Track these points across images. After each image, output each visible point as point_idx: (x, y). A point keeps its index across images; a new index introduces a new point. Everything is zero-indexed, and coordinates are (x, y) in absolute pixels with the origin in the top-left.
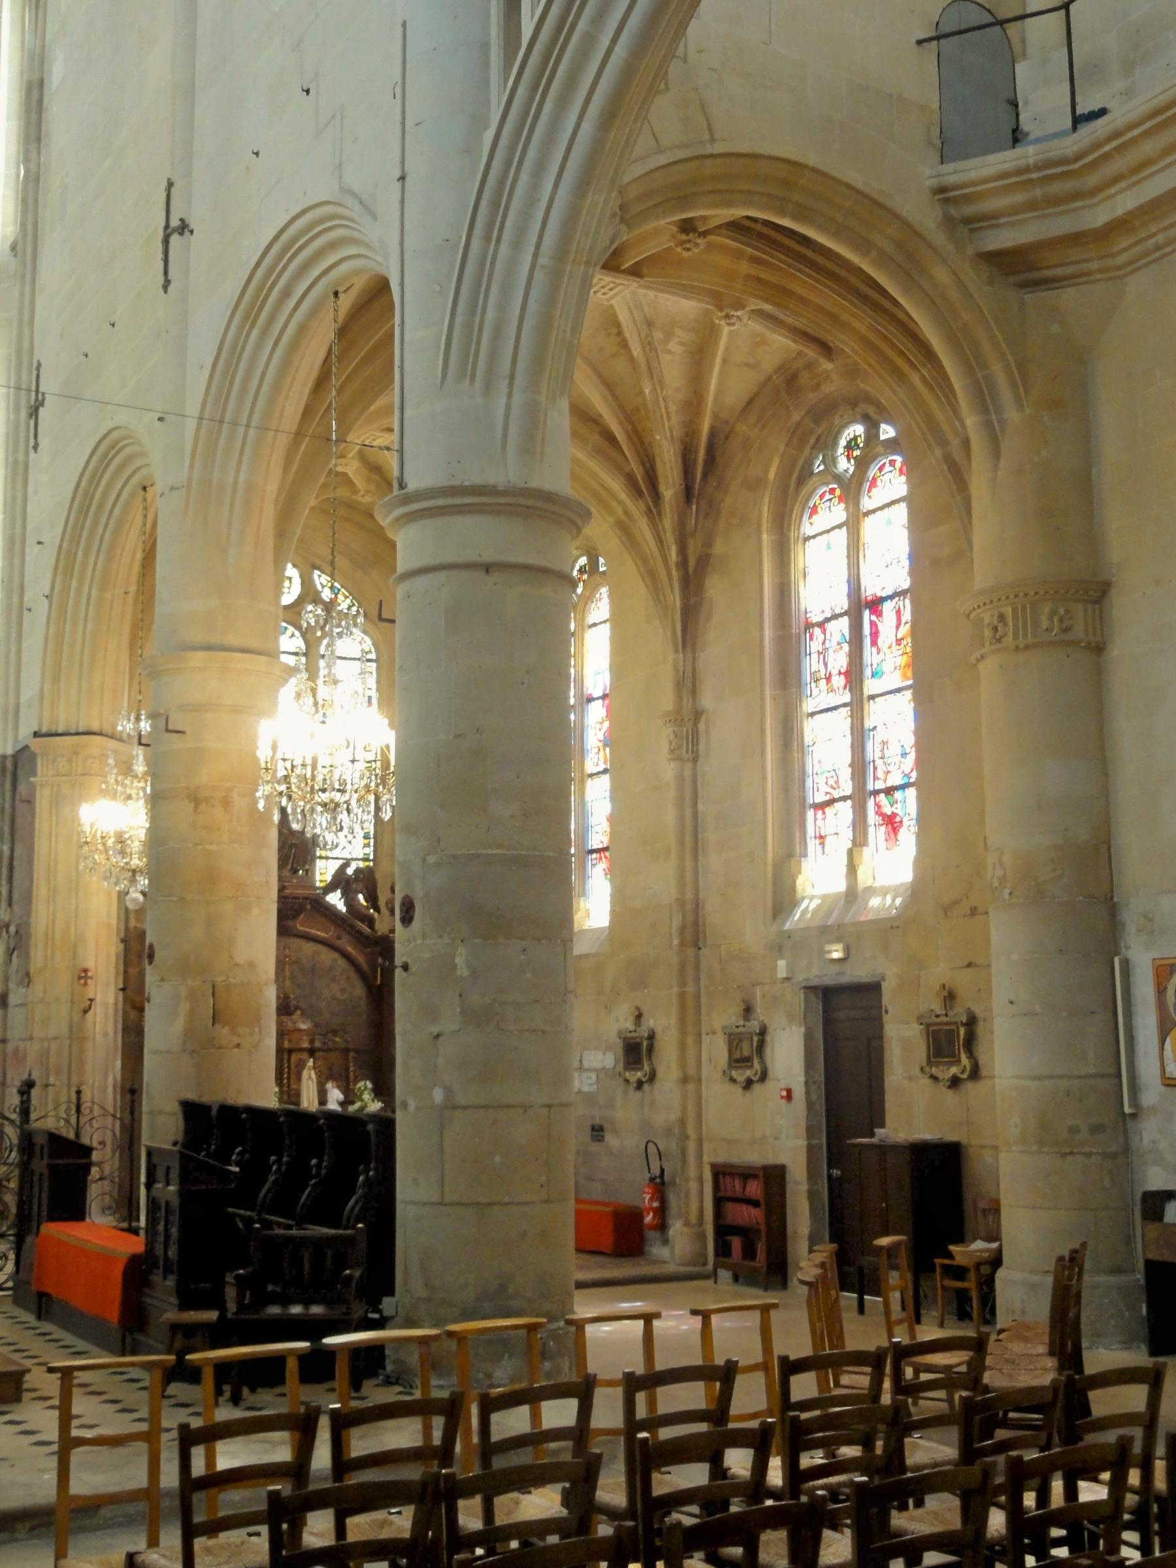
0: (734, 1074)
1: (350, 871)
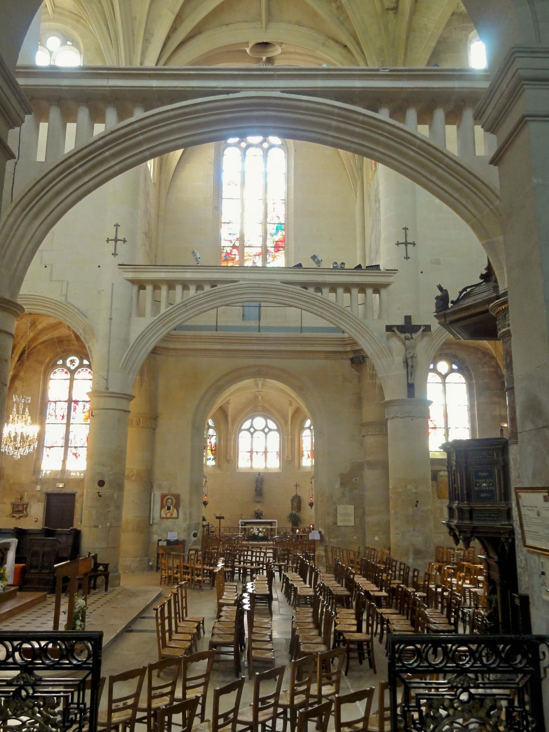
0: (14, 515)
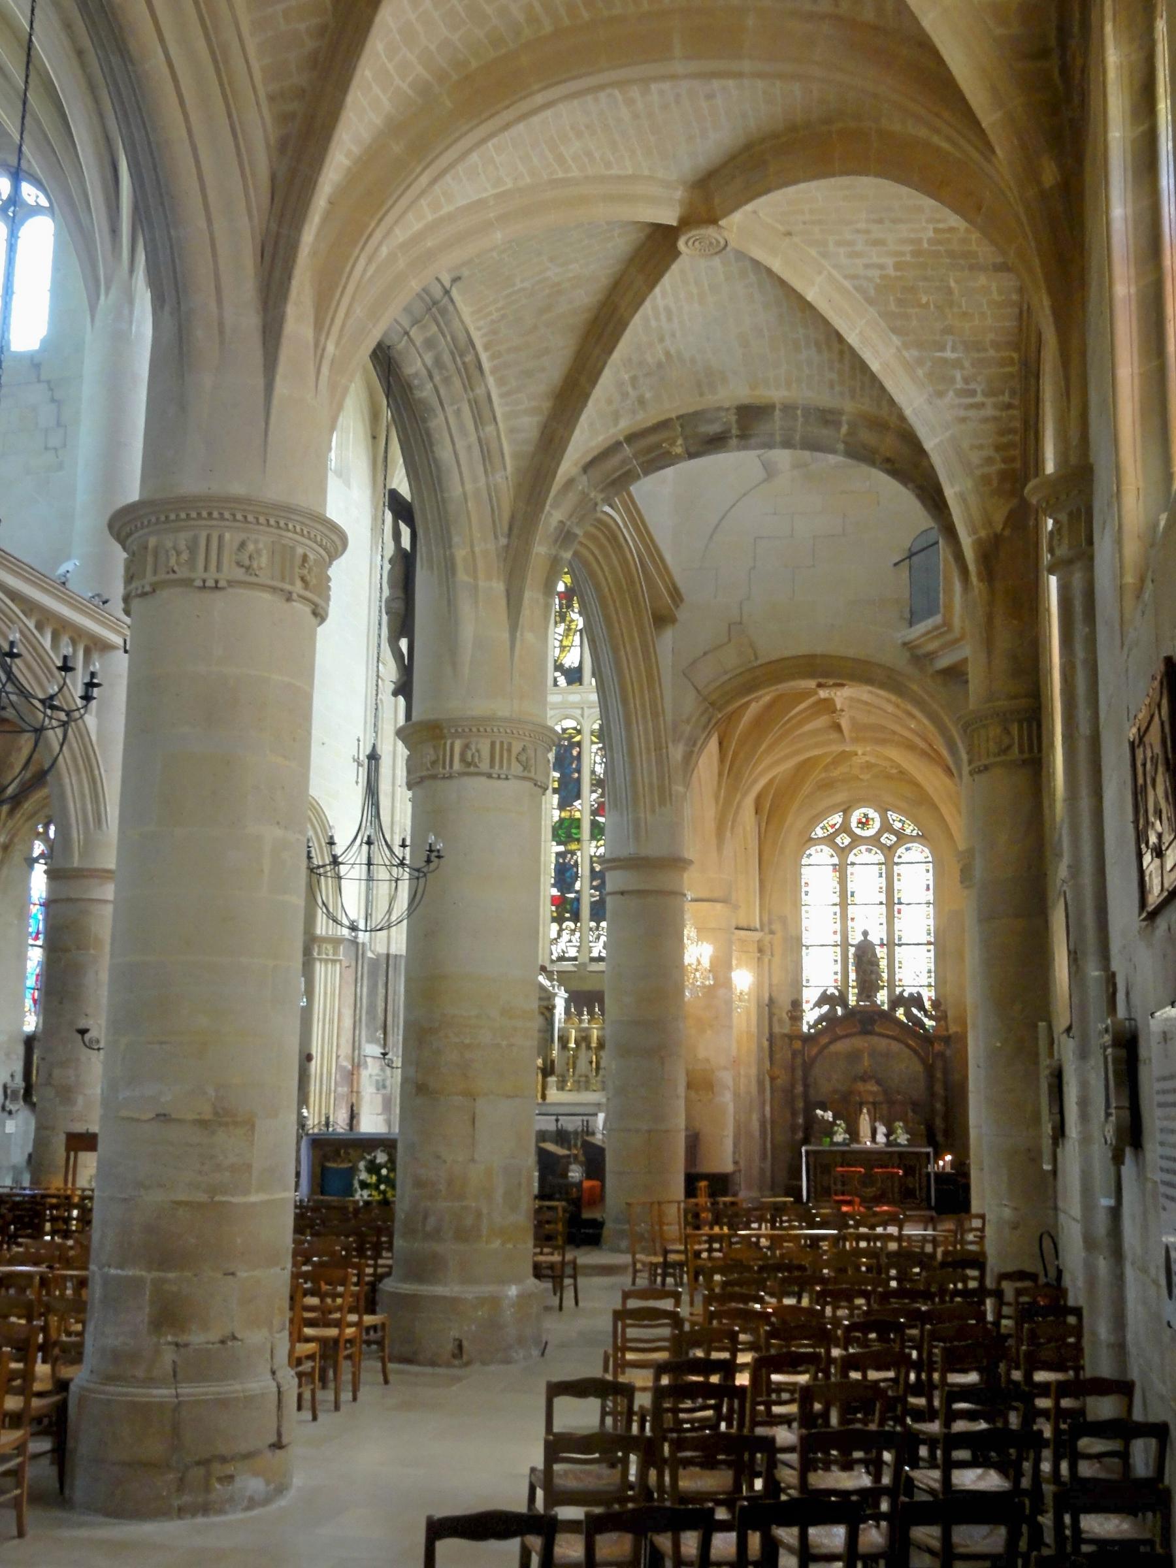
1: (906, 994)
